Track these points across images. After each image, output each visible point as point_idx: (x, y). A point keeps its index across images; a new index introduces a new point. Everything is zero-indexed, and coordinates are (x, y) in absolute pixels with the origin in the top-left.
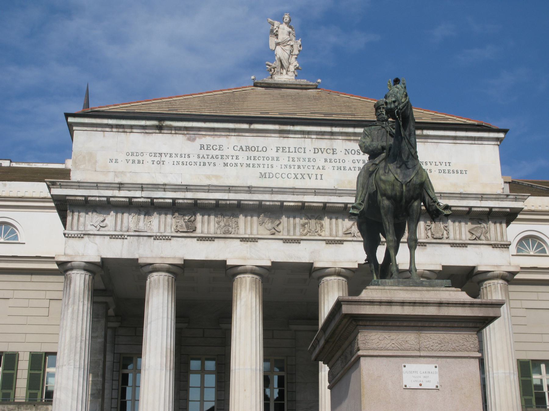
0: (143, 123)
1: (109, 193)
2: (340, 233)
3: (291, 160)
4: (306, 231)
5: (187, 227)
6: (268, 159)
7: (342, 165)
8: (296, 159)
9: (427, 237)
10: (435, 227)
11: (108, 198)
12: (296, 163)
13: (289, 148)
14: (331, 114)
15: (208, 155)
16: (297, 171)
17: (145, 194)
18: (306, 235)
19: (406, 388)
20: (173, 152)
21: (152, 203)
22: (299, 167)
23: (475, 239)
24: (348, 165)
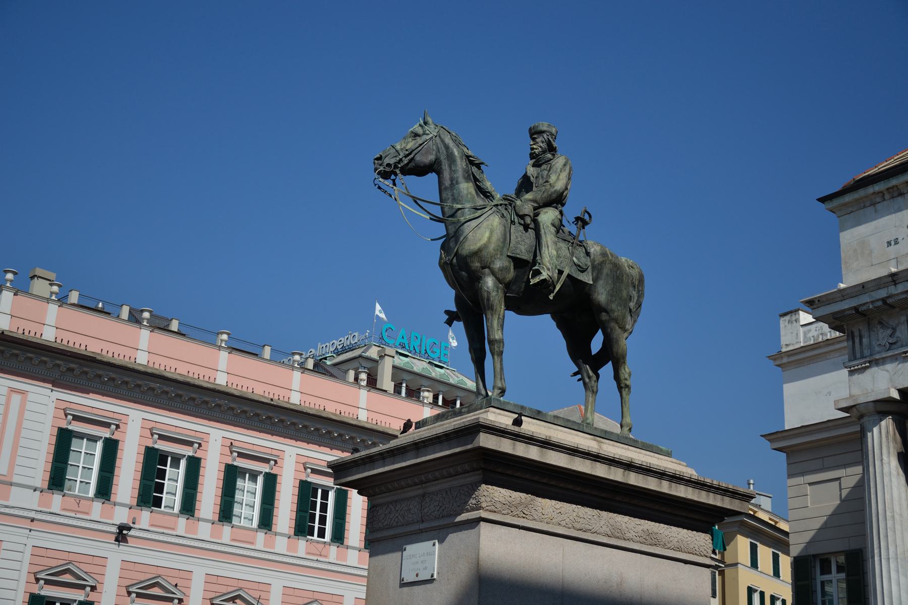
1: (882, 293)
11: (884, 300)
19: (403, 585)
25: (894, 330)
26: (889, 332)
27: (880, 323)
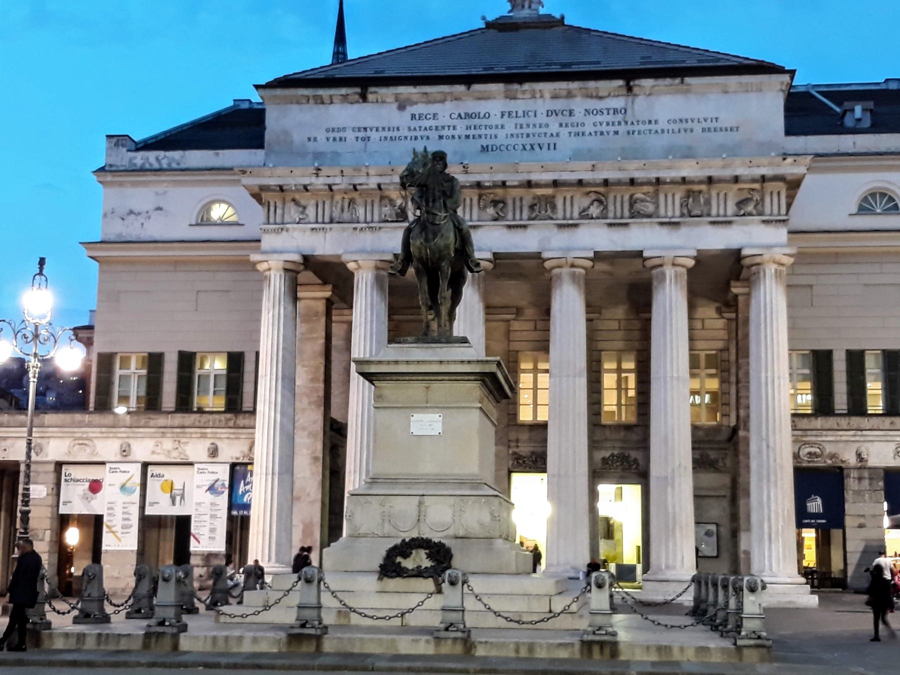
0: (343, 91)
2: (576, 214)
3: (518, 126)
4: (534, 215)
5: (397, 215)
6: (491, 127)
7: (580, 129)
8: (525, 126)
9: (682, 215)
10: (693, 201)
12: (526, 131)
13: (516, 112)
14: (570, 65)
15: (420, 127)
16: (525, 141)
17: (346, 180)
18: (533, 219)
20: (380, 125)
21: (355, 189)
22: (528, 135)
23: (744, 215)
24: (589, 128)
25: (305, 208)
26: (301, 209)
27: (294, 200)
